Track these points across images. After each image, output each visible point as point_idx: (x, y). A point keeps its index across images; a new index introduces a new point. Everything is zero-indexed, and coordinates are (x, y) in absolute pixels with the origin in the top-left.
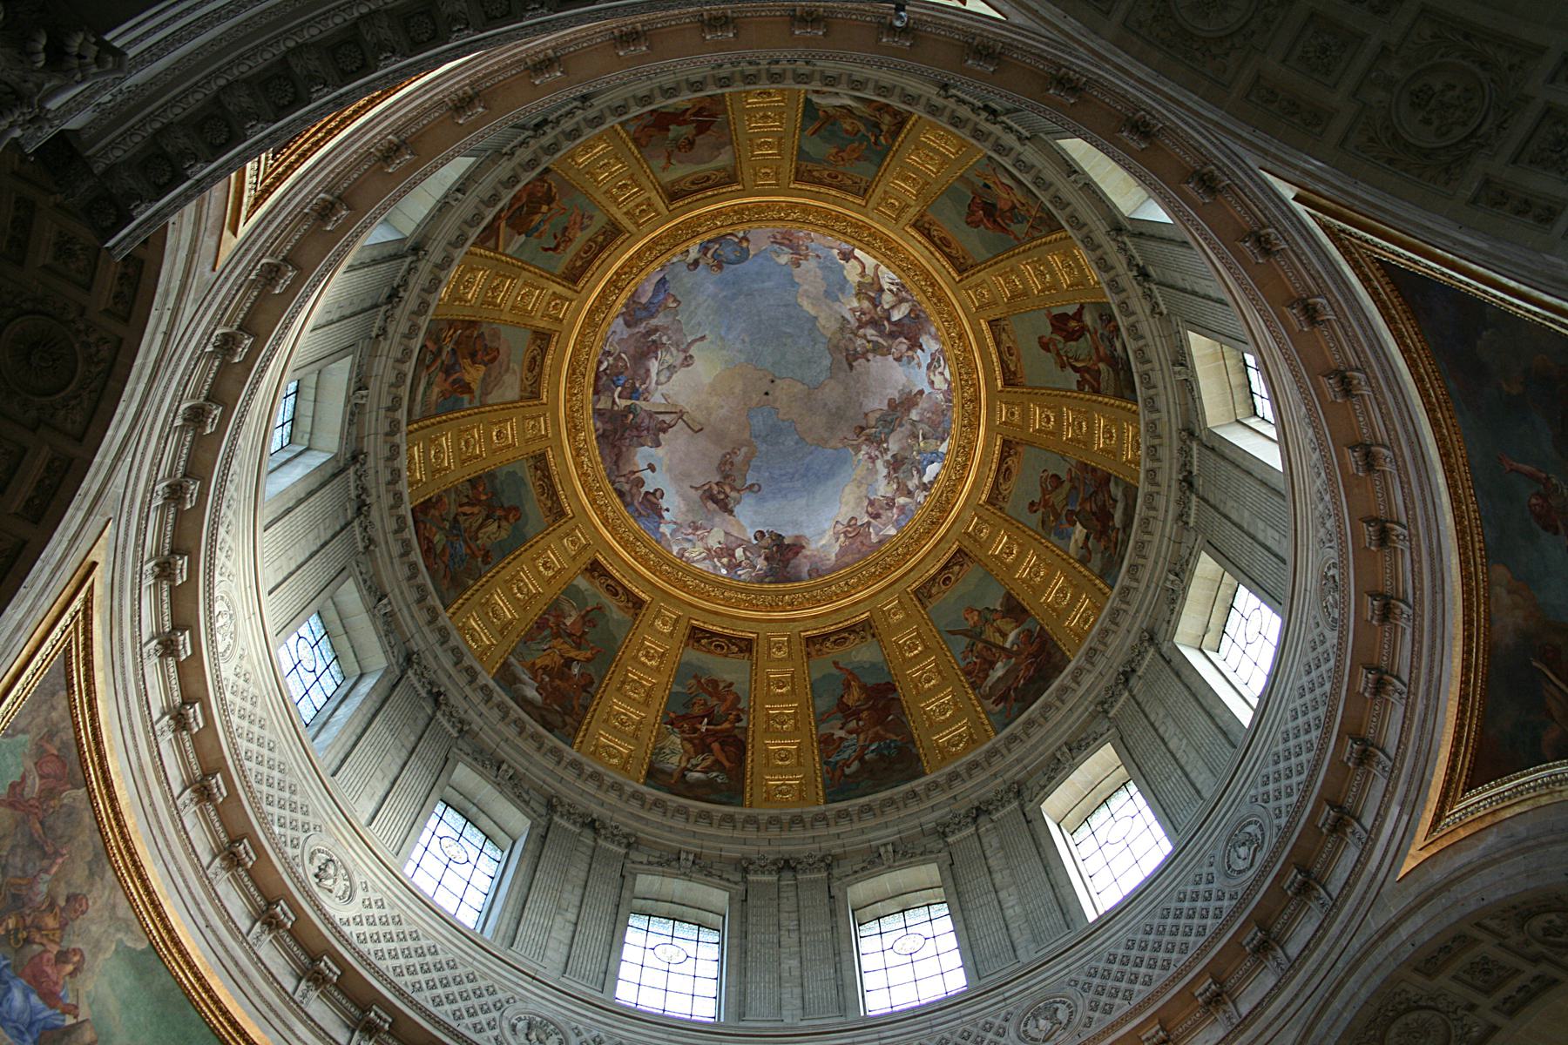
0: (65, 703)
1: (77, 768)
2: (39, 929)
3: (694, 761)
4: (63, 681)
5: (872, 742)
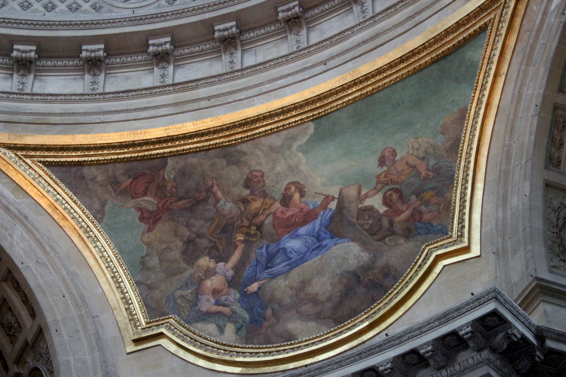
0: (93, 169)
1: (149, 163)
2: (256, 215)
4: (74, 169)
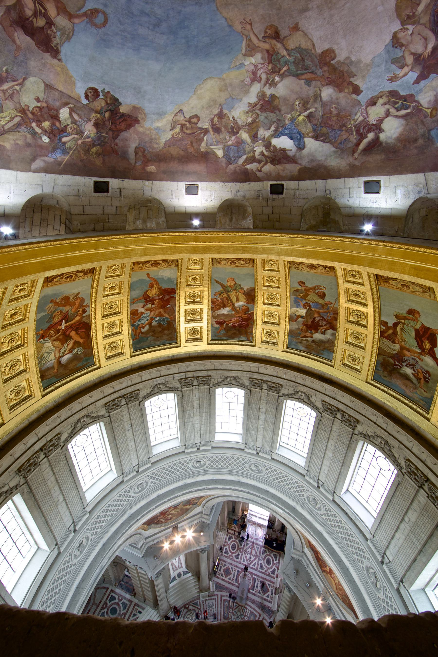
3: (62, 350)
5: (156, 317)
